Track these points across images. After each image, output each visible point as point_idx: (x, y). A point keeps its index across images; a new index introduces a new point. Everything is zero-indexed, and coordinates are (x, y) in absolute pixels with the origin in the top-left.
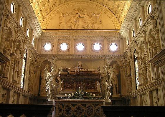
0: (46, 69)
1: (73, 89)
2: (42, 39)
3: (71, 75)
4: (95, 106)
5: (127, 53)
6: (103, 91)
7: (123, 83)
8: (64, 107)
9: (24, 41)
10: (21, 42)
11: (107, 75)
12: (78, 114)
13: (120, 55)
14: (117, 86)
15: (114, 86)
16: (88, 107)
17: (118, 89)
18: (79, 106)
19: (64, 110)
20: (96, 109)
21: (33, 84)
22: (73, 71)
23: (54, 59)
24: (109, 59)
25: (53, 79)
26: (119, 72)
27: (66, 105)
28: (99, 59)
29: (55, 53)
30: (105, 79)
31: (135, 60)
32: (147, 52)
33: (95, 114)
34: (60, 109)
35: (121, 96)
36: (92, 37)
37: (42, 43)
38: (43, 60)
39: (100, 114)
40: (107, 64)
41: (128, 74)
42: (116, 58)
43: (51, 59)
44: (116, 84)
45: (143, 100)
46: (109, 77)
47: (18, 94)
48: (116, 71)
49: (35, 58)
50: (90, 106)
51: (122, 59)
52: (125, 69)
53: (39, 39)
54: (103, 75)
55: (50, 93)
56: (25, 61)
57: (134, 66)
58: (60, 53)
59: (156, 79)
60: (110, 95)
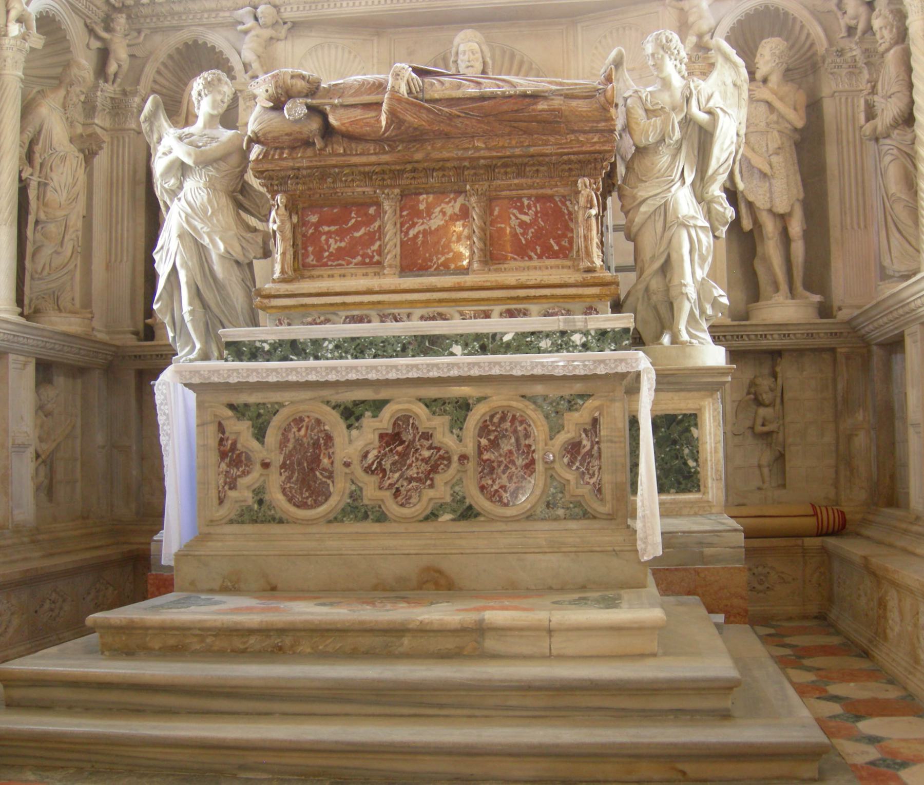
0: (156, 106)
1: (374, 264)
3: (351, 137)
6: (657, 265)
7: (842, 202)
8: (272, 436)
11: (688, 121)
14: (796, 227)
15: (770, 227)
16: (484, 430)
17: (798, 249)
18: (403, 420)
19: (266, 465)
20: (562, 438)
22: (367, 106)
23: (250, 23)
25: (211, 185)
26: (814, 107)
27: (283, 413)
30: (663, 159)
39: (598, 490)
41: (889, 110)
44: (781, 208)
48: (781, 99)
49: (91, 31)
50: (503, 419)
55: (186, 308)
60: (715, 303)
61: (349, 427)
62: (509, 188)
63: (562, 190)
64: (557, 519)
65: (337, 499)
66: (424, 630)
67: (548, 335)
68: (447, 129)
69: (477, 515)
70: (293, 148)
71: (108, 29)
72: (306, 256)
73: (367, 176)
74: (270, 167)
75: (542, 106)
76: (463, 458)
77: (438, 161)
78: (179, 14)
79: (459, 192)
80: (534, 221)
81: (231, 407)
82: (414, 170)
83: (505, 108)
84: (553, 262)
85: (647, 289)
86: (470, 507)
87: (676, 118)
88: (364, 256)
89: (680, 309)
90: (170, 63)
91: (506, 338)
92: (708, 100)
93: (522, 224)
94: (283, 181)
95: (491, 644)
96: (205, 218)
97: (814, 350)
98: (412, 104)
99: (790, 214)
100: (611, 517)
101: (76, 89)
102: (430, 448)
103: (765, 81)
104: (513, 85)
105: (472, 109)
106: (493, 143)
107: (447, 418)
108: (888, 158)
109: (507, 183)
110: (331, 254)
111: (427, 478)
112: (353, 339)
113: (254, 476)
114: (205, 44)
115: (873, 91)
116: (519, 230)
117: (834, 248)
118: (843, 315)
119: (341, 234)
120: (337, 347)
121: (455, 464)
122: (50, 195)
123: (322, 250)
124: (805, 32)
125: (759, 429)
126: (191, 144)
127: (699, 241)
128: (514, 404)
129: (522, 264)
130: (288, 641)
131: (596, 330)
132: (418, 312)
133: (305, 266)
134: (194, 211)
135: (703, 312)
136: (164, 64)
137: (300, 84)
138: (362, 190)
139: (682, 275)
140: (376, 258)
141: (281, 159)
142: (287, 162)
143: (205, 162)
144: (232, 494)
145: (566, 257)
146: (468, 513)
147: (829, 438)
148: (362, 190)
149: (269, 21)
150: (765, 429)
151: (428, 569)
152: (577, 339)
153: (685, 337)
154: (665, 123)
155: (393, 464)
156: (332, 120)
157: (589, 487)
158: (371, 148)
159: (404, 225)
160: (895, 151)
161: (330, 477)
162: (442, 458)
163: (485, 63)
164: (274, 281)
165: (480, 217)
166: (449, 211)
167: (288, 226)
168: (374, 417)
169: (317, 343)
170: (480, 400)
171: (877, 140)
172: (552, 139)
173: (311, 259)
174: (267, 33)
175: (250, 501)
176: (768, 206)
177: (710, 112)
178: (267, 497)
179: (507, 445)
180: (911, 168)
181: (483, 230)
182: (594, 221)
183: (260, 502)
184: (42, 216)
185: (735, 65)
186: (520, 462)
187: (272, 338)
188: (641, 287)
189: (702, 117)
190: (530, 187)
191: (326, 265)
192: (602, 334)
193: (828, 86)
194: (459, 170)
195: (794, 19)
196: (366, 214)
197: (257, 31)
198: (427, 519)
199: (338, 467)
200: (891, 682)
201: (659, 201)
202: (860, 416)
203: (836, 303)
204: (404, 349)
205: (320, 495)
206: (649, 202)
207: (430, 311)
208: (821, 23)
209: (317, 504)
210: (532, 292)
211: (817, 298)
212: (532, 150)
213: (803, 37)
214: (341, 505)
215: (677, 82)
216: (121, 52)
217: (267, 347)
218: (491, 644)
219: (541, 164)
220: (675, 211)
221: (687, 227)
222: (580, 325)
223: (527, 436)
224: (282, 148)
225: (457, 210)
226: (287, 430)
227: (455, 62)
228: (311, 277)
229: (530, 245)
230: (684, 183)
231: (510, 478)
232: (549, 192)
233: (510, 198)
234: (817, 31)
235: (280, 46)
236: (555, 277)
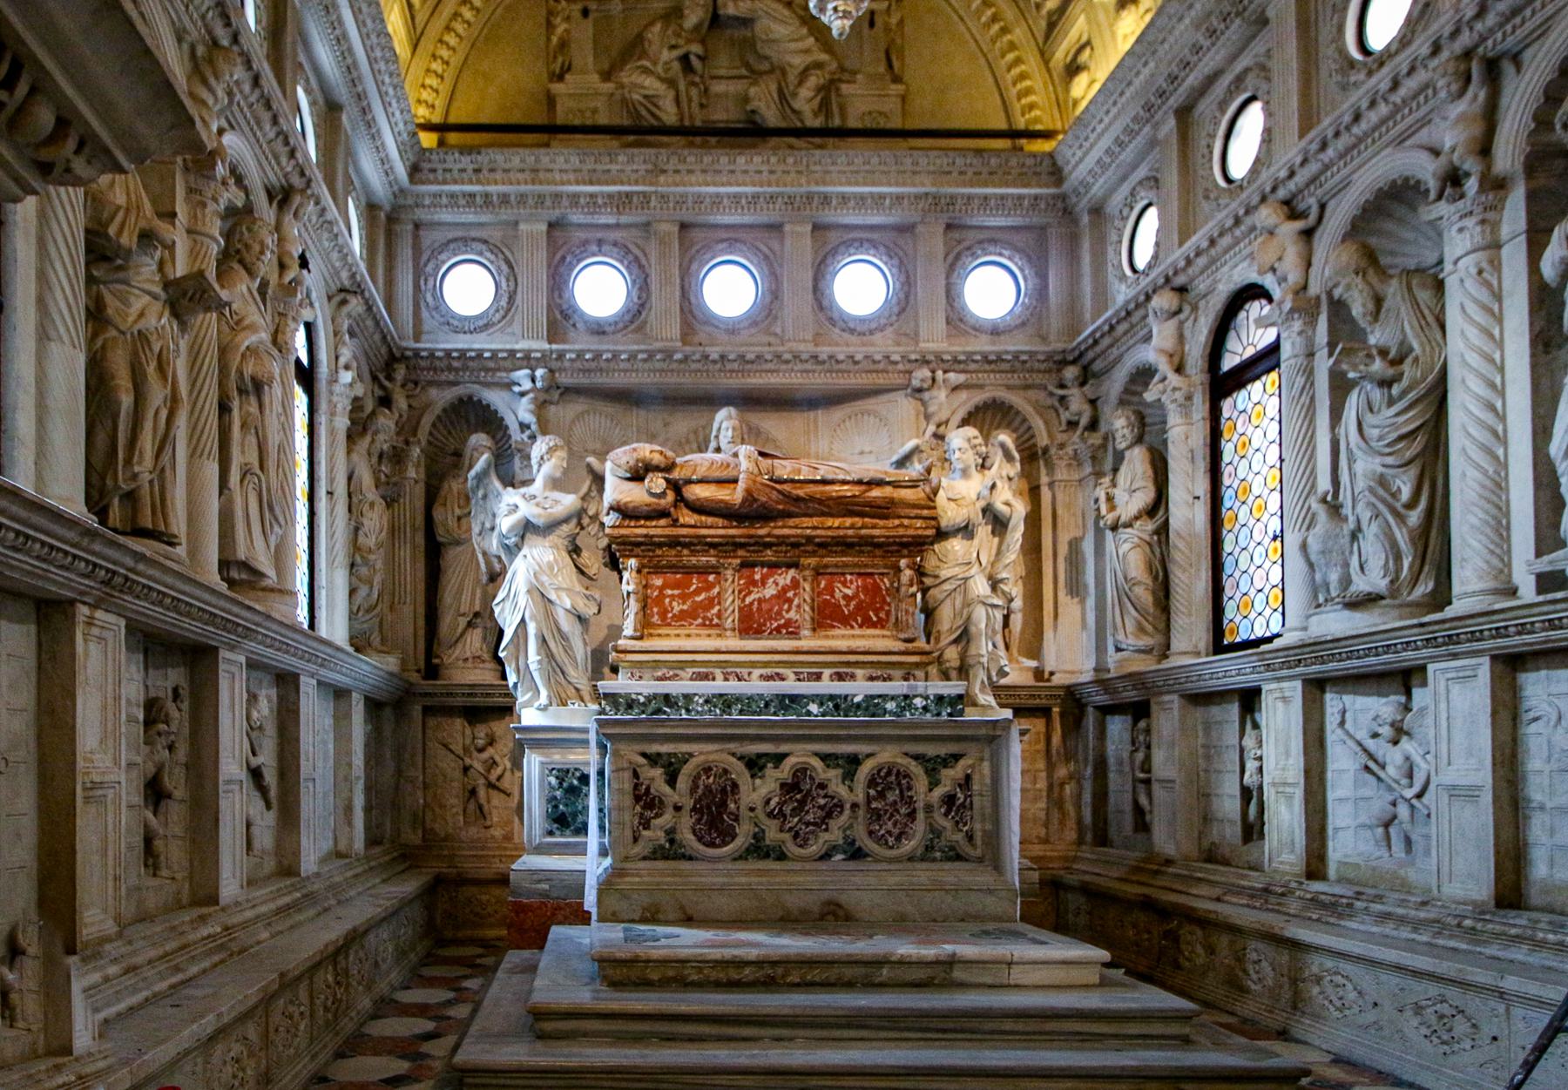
3: (699, 508)
4: (933, 767)
8: (683, 782)
12: (796, 836)
16: (872, 783)
18: (801, 772)
19: (678, 808)
20: (939, 792)
24: (956, 388)
27: (693, 762)
33: (936, 832)
34: (646, 801)
36: (826, 199)
39: (970, 837)
42: (1015, 380)
50: (889, 773)
51: (1062, 386)
61: (753, 776)
64: (934, 860)
65: (740, 842)
67: (893, 698)
69: (867, 855)
76: (855, 806)
80: (856, 595)
81: (644, 755)
86: (860, 849)
88: (704, 618)
89: (976, 676)
91: (856, 700)
93: (845, 597)
100: (980, 860)
102: (825, 796)
104: (848, 473)
107: (839, 771)
108: (1126, 547)
111: (823, 823)
113: (667, 819)
116: (843, 602)
118: (1057, 680)
119: (683, 598)
120: (707, 702)
121: (847, 812)
128: (899, 760)
132: (757, 672)
139: (979, 648)
145: (883, 627)
146: (857, 854)
152: (918, 702)
155: (793, 810)
158: (720, 522)
161: (737, 819)
162: (836, 805)
166: (781, 582)
168: (776, 767)
169: (688, 698)
170: (869, 756)
173: (656, 619)
179: (892, 796)
186: (903, 811)
187: (646, 692)
192: (940, 699)
196: (706, 581)
199: (744, 812)
204: (767, 705)
205: (728, 835)
207: (769, 671)
209: (725, 844)
222: (920, 691)
223: (910, 788)
225: (788, 581)
226: (697, 778)
229: (852, 616)
231: (895, 824)
236: (881, 644)
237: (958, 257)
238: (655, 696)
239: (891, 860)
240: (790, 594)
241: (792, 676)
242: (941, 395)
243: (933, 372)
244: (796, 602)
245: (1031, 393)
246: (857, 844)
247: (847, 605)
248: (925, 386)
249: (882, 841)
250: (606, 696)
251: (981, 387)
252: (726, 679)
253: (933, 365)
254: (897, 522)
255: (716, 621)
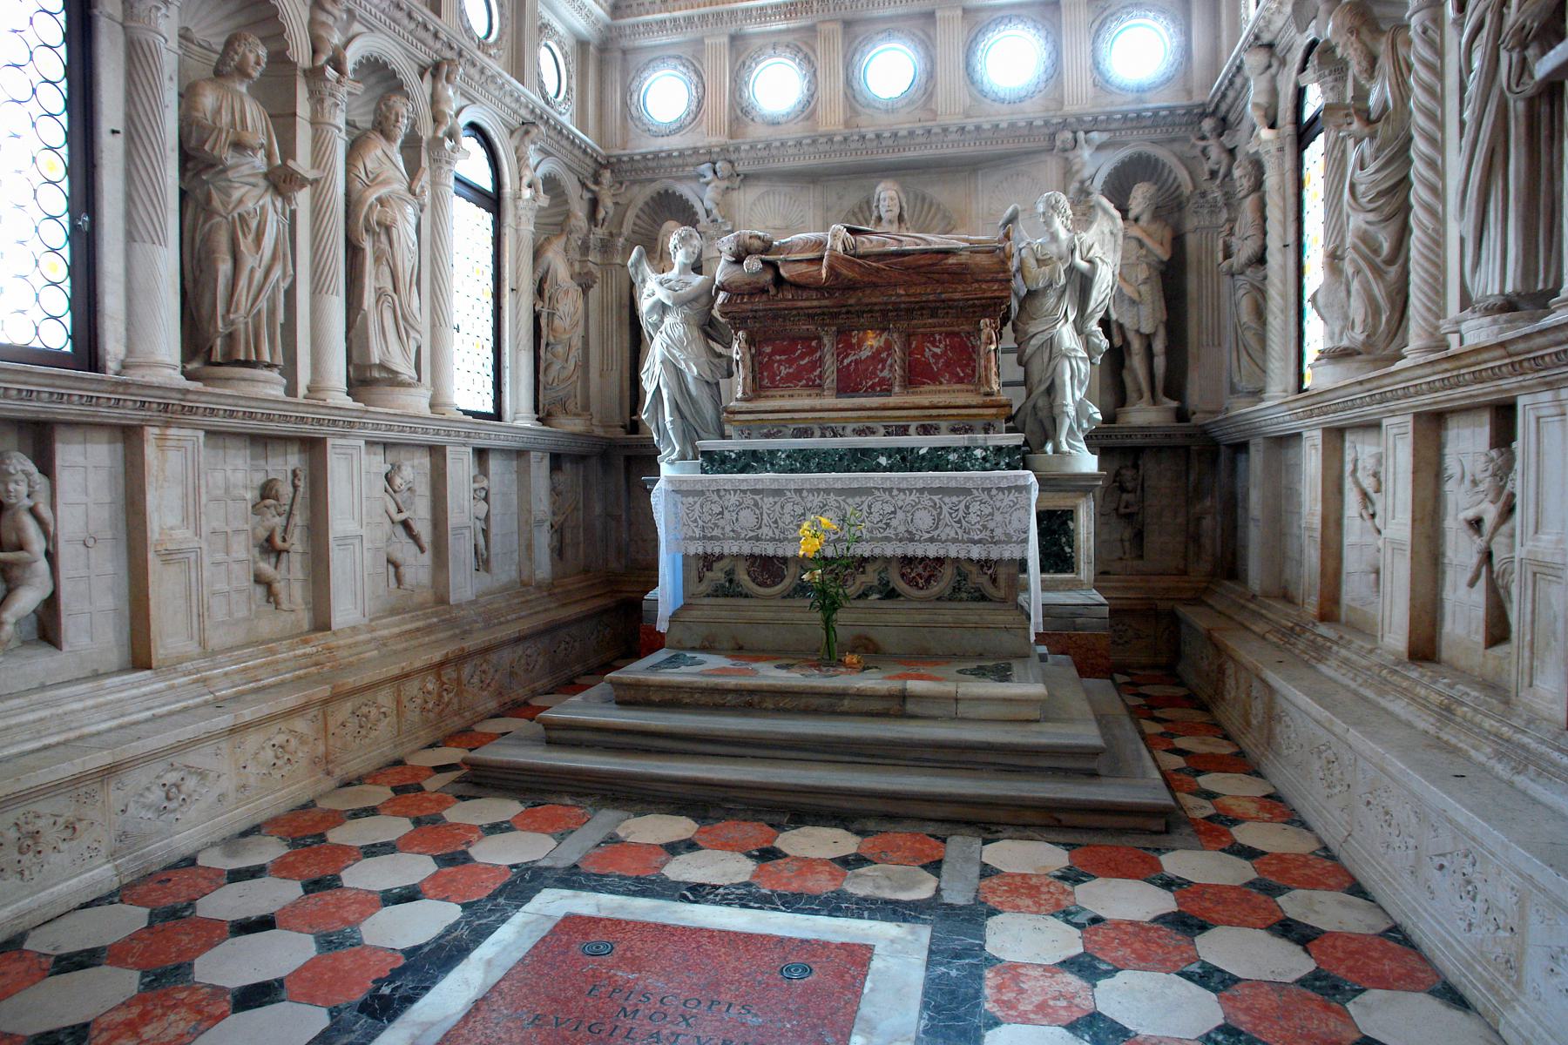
1: (816, 386)
2: (625, 43)
3: (797, 286)
5: (1238, 81)
6: (1043, 387)
9: (435, 70)
10: (408, 73)
11: (1072, 269)
13: (1189, 111)
14: (1159, 345)
15: (1136, 344)
17: (1160, 363)
21: (585, 364)
23: (710, 176)
24: (1100, 147)
25: (686, 321)
26: (1178, 242)
28: (1028, 154)
29: (717, 140)
30: (1051, 301)
31: (1304, 134)
32: (1431, 44)
35: (1182, 415)
37: (625, 72)
38: (641, 195)
39: (994, 580)
40: (1082, 182)
41: (1244, 250)
42: (1158, 135)
43: (694, 185)
44: (1146, 328)
45: (1348, 468)
46: (1083, 283)
47: (437, 452)
48: (1150, 235)
49: (584, 185)
51: (1203, 138)
52: (1224, 215)
53: (603, 48)
54: (1038, 275)
55: (668, 418)
56: (489, 217)
57: (1290, 190)
58: (756, 132)
59: (1508, 305)
60: (1090, 419)
62: (924, 326)
63: (966, 328)
64: (961, 600)
66: (860, 695)
67: (955, 450)
68: (874, 279)
69: (899, 595)
70: (751, 295)
71: (597, 182)
72: (762, 379)
73: (811, 317)
74: (734, 309)
75: (951, 260)
77: (867, 305)
78: (653, 169)
79: (884, 330)
80: (944, 353)
82: (848, 312)
83: (922, 262)
84: (958, 387)
85: (1034, 407)
86: (893, 589)
87: (1062, 268)
89: (1062, 424)
90: (646, 209)
91: (921, 452)
92: (1088, 252)
93: (935, 355)
94: (744, 320)
95: (910, 707)
96: (682, 348)
97: (1169, 447)
98: (849, 261)
99: (1154, 334)
100: (1003, 601)
101: (575, 236)
103: (1136, 220)
104: (928, 243)
105: (896, 264)
106: (912, 291)
108: (1241, 292)
109: (923, 323)
110: (782, 378)
112: (801, 450)
114: (674, 193)
115: (1231, 233)
116: (932, 360)
117: (1190, 361)
119: (790, 362)
120: (788, 456)
122: (557, 322)
123: (775, 375)
124: (1173, 176)
125: (1122, 510)
126: (669, 288)
127: (1079, 369)
129: (932, 388)
130: (756, 699)
131: (994, 447)
132: (850, 427)
133: (761, 387)
134: (674, 343)
135: (1080, 425)
136: (641, 209)
137: (757, 243)
138: (806, 327)
139: (1064, 397)
140: (818, 381)
141: (742, 303)
142: (746, 305)
143: (682, 302)
144: (709, 574)
145: (969, 382)
146: (891, 594)
147: (1181, 519)
148: (806, 327)
149: (726, 173)
150: (1128, 511)
151: (859, 637)
152: (979, 453)
153: (1065, 448)
154: (1053, 271)
156: (782, 271)
157: (987, 577)
159: (840, 355)
160: (1248, 286)
163: (901, 208)
164: (737, 400)
165: (901, 350)
167: (748, 356)
169: (772, 453)
171: (1233, 275)
172: (960, 288)
174: (725, 184)
175: (722, 581)
176: (1136, 327)
177: (1090, 261)
178: (736, 577)
180: (1260, 300)
181: (903, 360)
182: (993, 354)
183: (731, 581)
184: (552, 340)
185: (1112, 218)
187: (737, 449)
188: (1030, 404)
189: (1084, 265)
190: (941, 326)
191: (777, 387)
192: (999, 450)
193: (1191, 222)
194: (884, 313)
195: (1164, 165)
196: (810, 346)
197: (716, 183)
198: (859, 597)
200: (1226, 737)
201: (1046, 336)
202: (1208, 503)
203: (1191, 408)
204: (841, 459)
206: (1038, 336)
207: (860, 425)
208: (1187, 168)
209: (774, 584)
210: (942, 412)
211: (1174, 404)
212: (943, 296)
213: (1171, 180)
214: (793, 585)
215: (1063, 235)
216: (607, 203)
217: (733, 456)
218: (910, 707)
219: (950, 307)
220: (1060, 343)
221: (1069, 358)
222: (980, 442)
224: (743, 295)
225: (882, 344)
227: (877, 207)
228: (767, 397)
230: (1067, 321)
231: (925, 568)
232: (956, 329)
233: (924, 335)
234: (1183, 175)
235: (735, 194)
236: (961, 399)
237: (1102, 24)
238: (745, 453)
239: (921, 600)
240: (884, 355)
241: (883, 431)
242: (1086, 153)
243: (1075, 133)
244: (889, 362)
245: (1177, 147)
246: (891, 585)
247: (936, 363)
248: (1068, 146)
249: (912, 582)
250: (704, 453)
251: (1124, 144)
252: (823, 435)
253: (1075, 127)
254: (976, 285)
255: (818, 381)
